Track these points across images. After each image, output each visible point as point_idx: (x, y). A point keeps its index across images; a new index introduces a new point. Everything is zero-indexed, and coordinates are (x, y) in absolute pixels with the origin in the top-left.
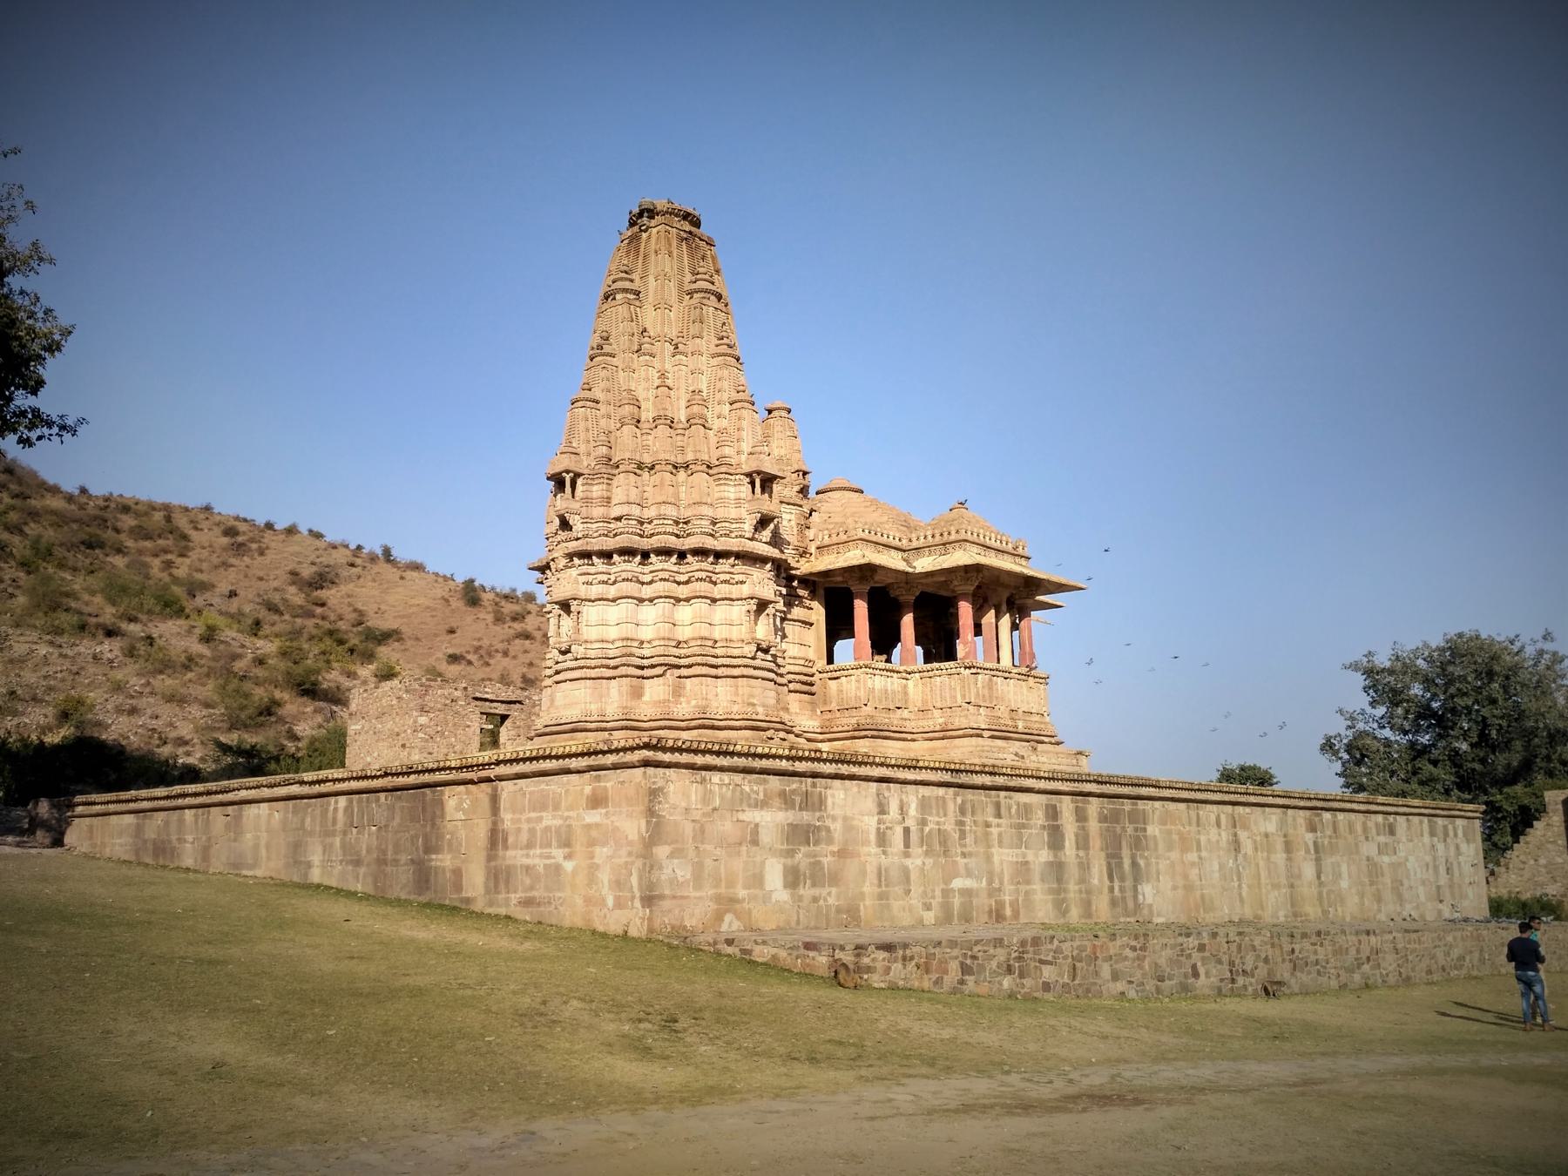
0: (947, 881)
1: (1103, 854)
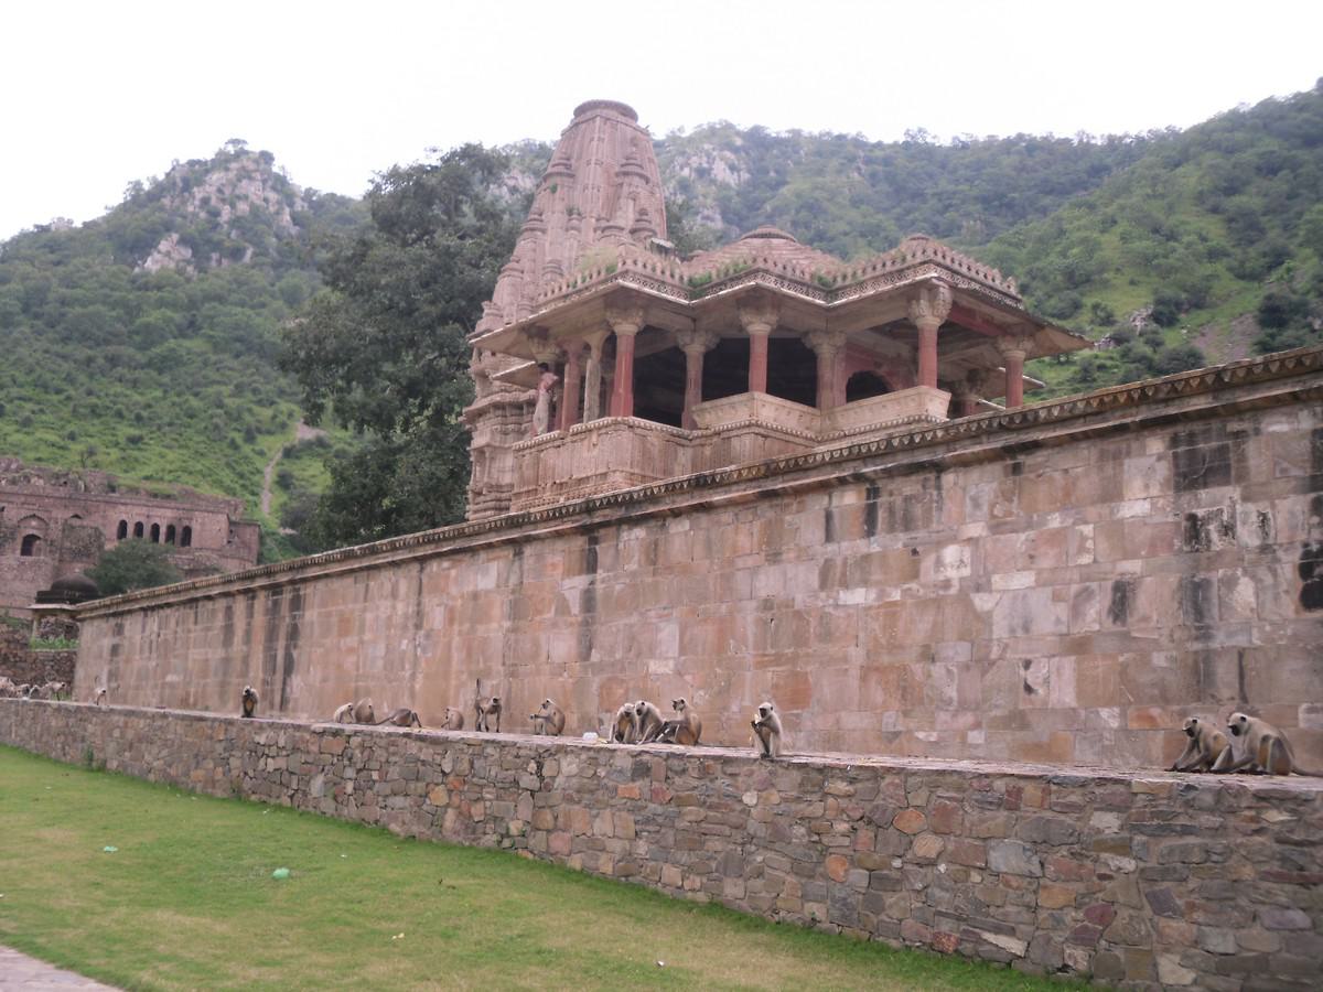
0: (164, 677)
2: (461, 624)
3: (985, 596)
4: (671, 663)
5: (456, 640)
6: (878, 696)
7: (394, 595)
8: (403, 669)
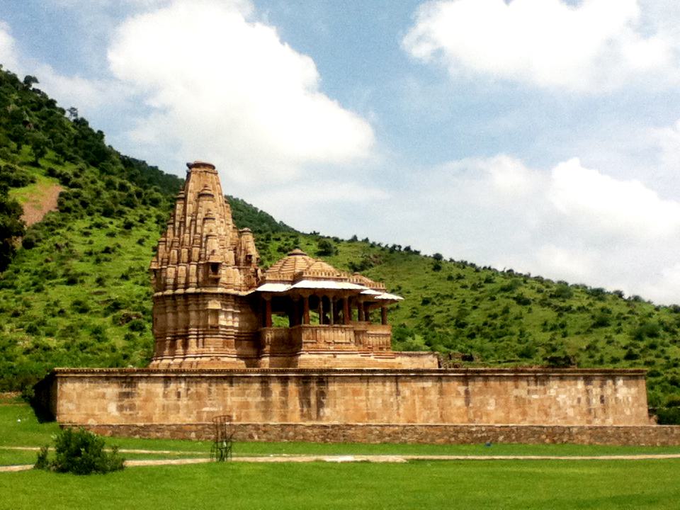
5: (417, 400)
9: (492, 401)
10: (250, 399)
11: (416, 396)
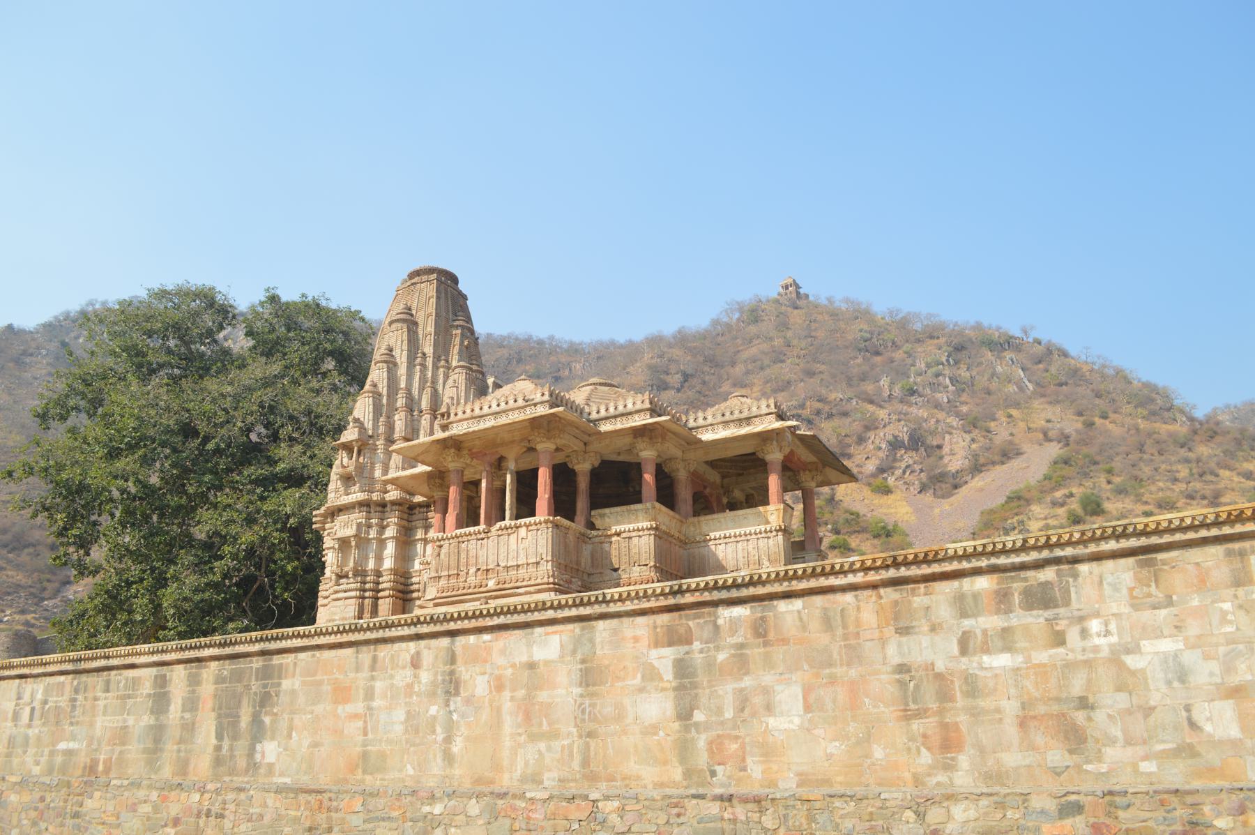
1: (213, 715)
2: (513, 690)
3: (1137, 657)
4: (797, 721)
5: (507, 706)
6: (1039, 740)
7: (416, 663)
8: (434, 732)
9: (789, 696)
10: (131, 721)
11: (507, 694)
